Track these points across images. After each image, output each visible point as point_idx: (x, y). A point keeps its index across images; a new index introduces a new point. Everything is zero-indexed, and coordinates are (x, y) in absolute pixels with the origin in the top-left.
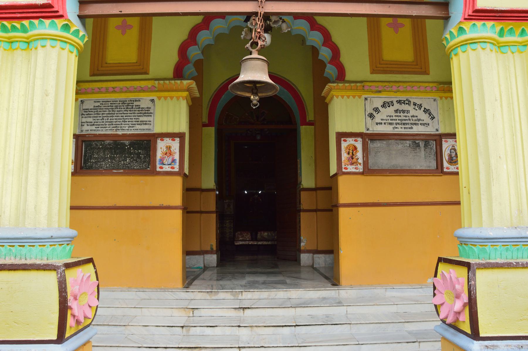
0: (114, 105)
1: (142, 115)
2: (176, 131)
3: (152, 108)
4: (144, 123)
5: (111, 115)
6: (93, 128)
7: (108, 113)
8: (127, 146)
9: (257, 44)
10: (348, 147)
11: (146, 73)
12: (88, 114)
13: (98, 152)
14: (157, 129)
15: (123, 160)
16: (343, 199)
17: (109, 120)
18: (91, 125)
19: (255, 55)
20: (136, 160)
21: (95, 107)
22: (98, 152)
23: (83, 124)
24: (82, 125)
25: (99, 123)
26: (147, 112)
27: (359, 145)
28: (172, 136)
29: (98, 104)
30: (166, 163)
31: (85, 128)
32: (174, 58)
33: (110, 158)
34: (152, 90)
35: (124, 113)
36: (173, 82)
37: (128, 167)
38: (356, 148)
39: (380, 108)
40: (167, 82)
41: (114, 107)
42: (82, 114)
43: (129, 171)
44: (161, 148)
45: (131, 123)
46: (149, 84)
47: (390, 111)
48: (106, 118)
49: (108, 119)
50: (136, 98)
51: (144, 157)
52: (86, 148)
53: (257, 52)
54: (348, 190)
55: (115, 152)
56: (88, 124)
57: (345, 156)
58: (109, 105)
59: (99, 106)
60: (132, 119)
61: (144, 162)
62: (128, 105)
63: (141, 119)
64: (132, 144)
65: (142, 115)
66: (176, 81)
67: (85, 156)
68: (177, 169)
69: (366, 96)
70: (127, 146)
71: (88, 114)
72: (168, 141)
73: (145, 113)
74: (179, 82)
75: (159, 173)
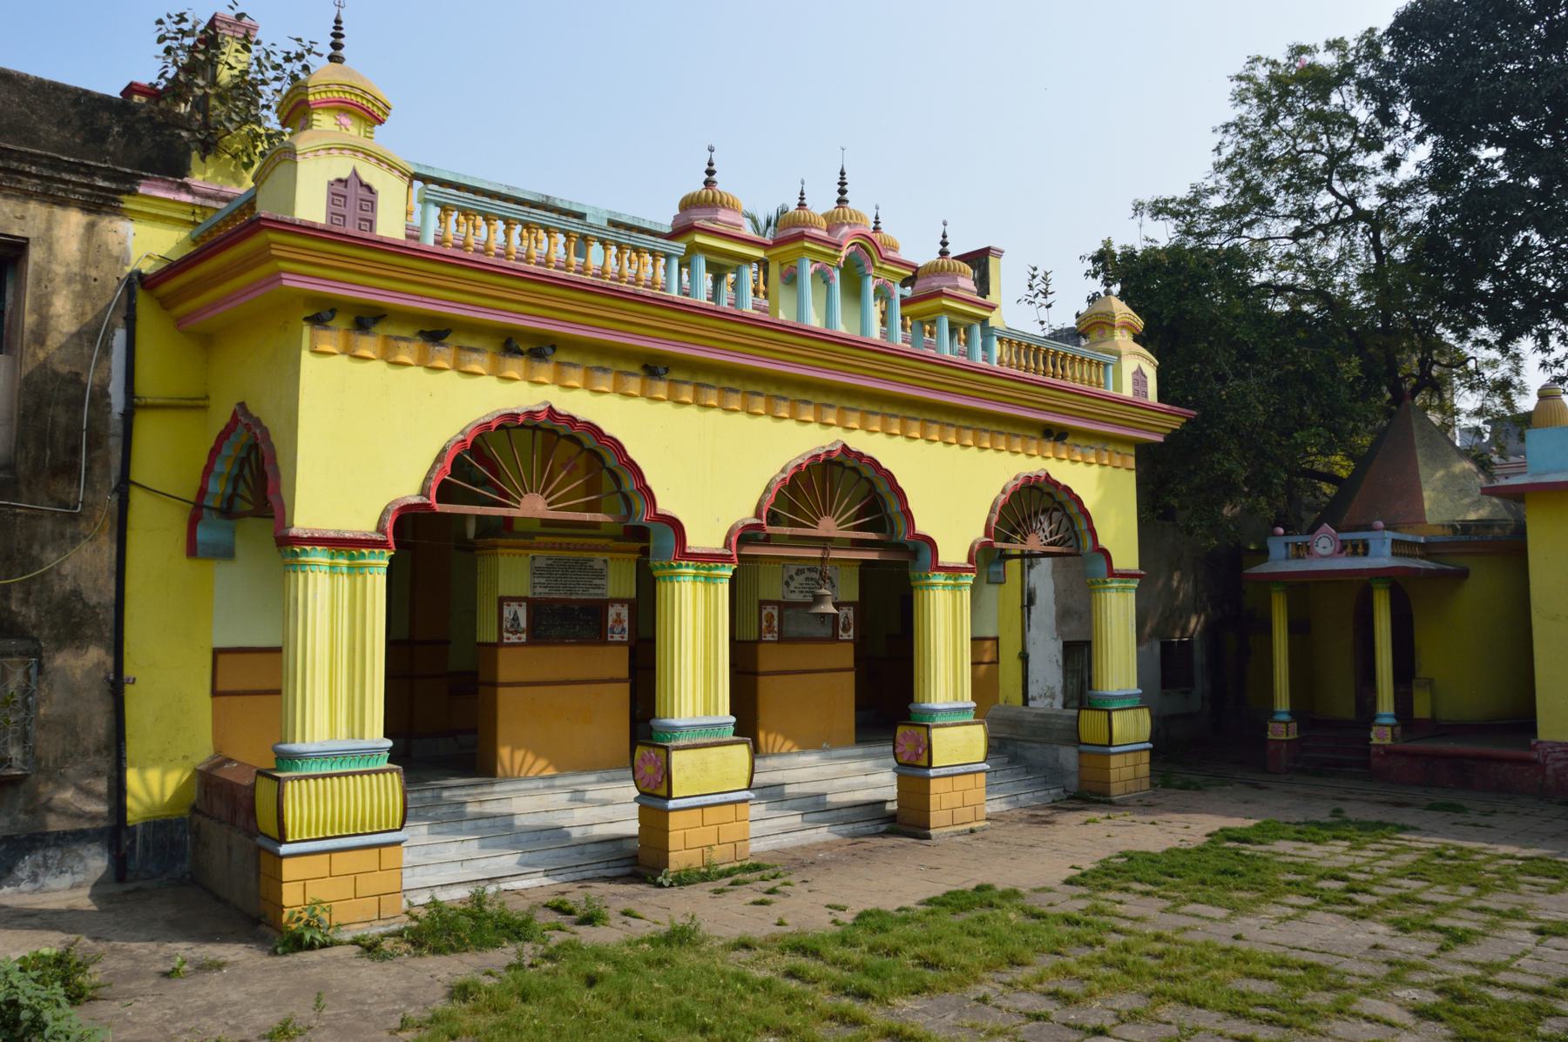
2: (627, 596)
16: (762, 667)
26: (600, 574)
27: (775, 613)
28: (621, 601)
31: (538, 590)
34: (604, 549)
43: (581, 641)
46: (603, 542)
47: (801, 579)
62: (582, 565)
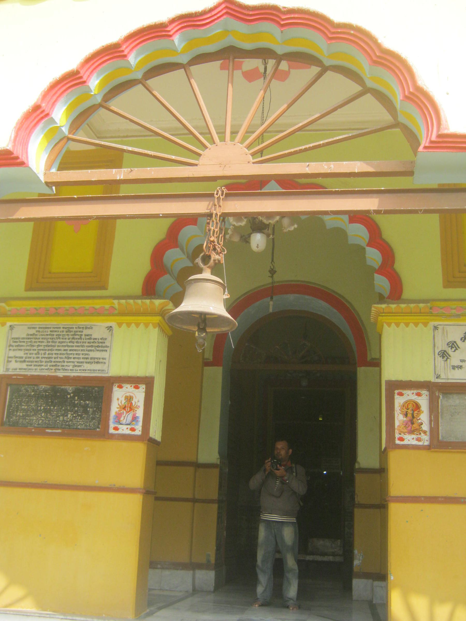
0: (55, 333)
1: (93, 349)
2: (141, 373)
3: (109, 339)
4: (96, 360)
5: (50, 348)
6: (24, 365)
7: (46, 344)
8: (69, 394)
9: (209, 257)
10: (405, 405)
11: (104, 288)
12: (18, 346)
13: (28, 402)
14: (114, 370)
15: (63, 415)
17: (47, 356)
18: (21, 362)
19: (207, 274)
20: (81, 416)
21: (28, 335)
22: (28, 402)
23: (10, 359)
24: (9, 362)
25: (32, 360)
26: (101, 345)
27: (424, 402)
28: (135, 381)
29: (33, 331)
30: (124, 422)
32: (145, 267)
33: (46, 411)
34: (111, 312)
35: (68, 346)
36: (139, 301)
37: (69, 425)
38: (417, 407)
39: (459, 343)
40: (131, 301)
41: (55, 337)
42: (10, 346)
43: (70, 431)
44: (118, 399)
45: (77, 360)
46: (107, 304)
48: (43, 352)
49: (45, 354)
50: (86, 323)
51: (94, 411)
52: (12, 395)
53: (209, 270)
54: (404, 476)
55: (52, 402)
56: (18, 359)
57: (399, 419)
58: (49, 333)
59: (34, 334)
60: (79, 354)
61: (93, 418)
62: (75, 334)
63: (92, 354)
64: (77, 392)
65: (93, 349)
66: (144, 301)
67: (10, 406)
68: (139, 431)
69: (436, 323)
70: (69, 394)
71: (18, 346)
72: (128, 389)
73: (98, 346)
74: (148, 301)
75: (112, 437)
